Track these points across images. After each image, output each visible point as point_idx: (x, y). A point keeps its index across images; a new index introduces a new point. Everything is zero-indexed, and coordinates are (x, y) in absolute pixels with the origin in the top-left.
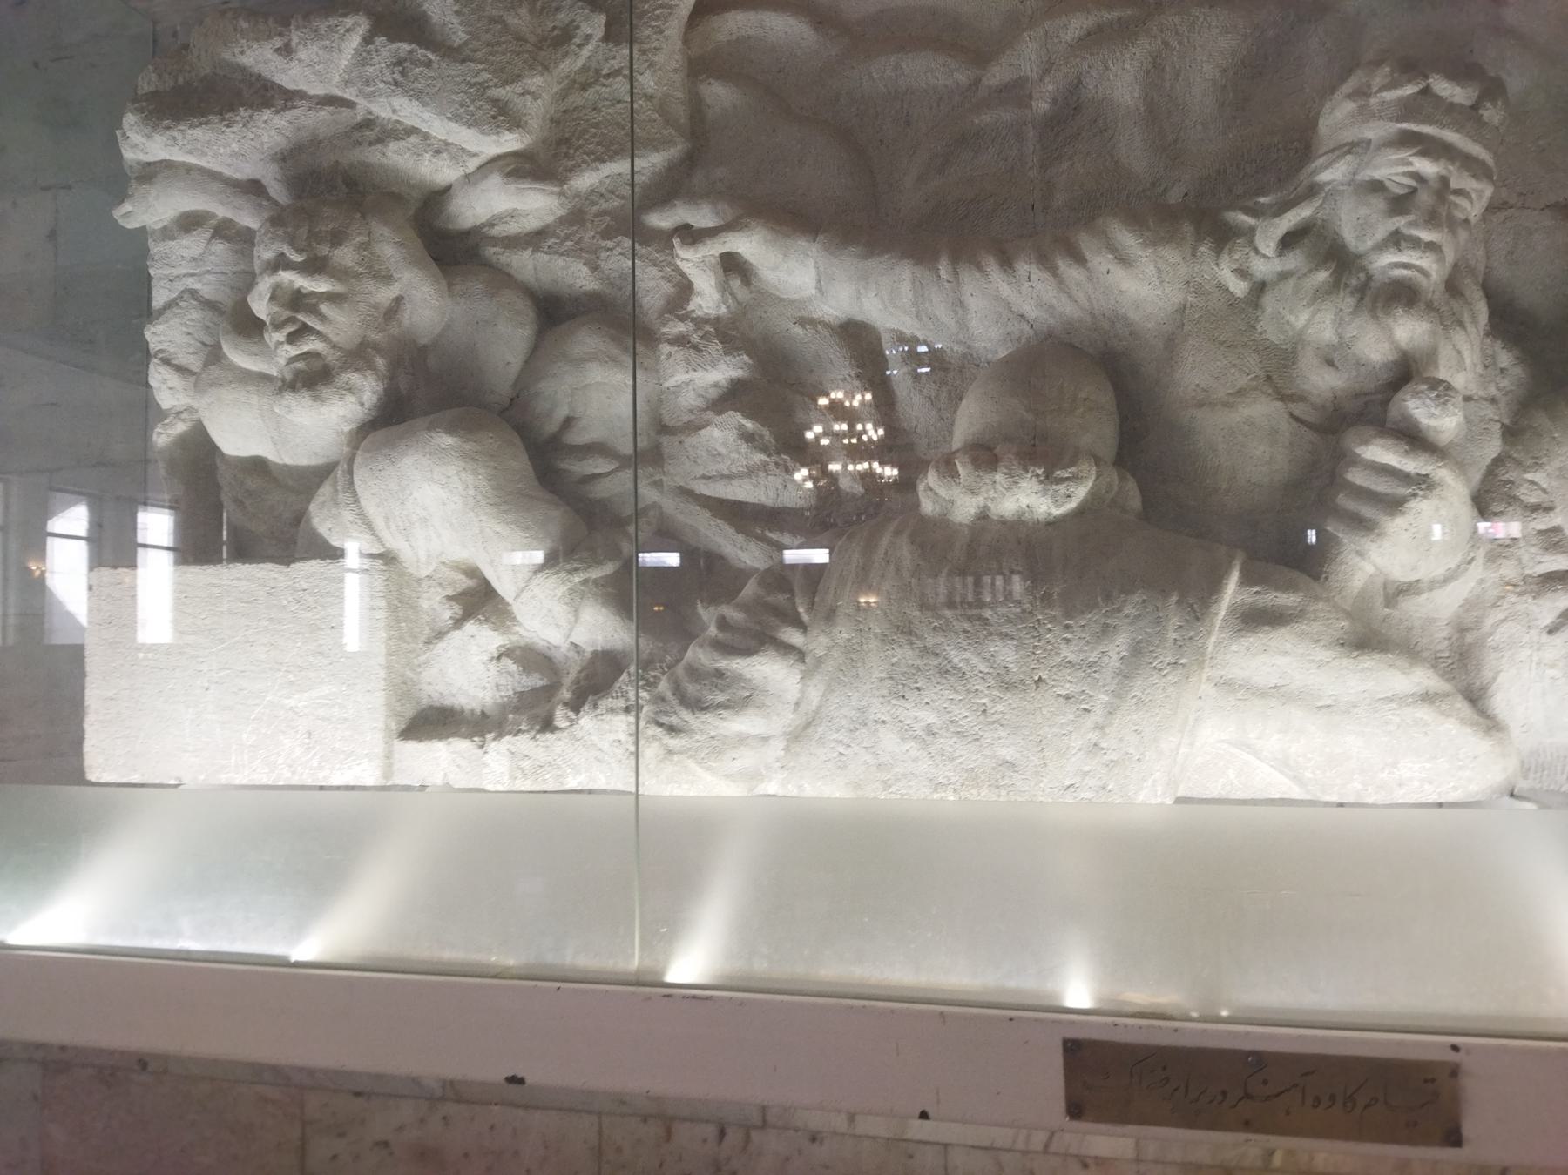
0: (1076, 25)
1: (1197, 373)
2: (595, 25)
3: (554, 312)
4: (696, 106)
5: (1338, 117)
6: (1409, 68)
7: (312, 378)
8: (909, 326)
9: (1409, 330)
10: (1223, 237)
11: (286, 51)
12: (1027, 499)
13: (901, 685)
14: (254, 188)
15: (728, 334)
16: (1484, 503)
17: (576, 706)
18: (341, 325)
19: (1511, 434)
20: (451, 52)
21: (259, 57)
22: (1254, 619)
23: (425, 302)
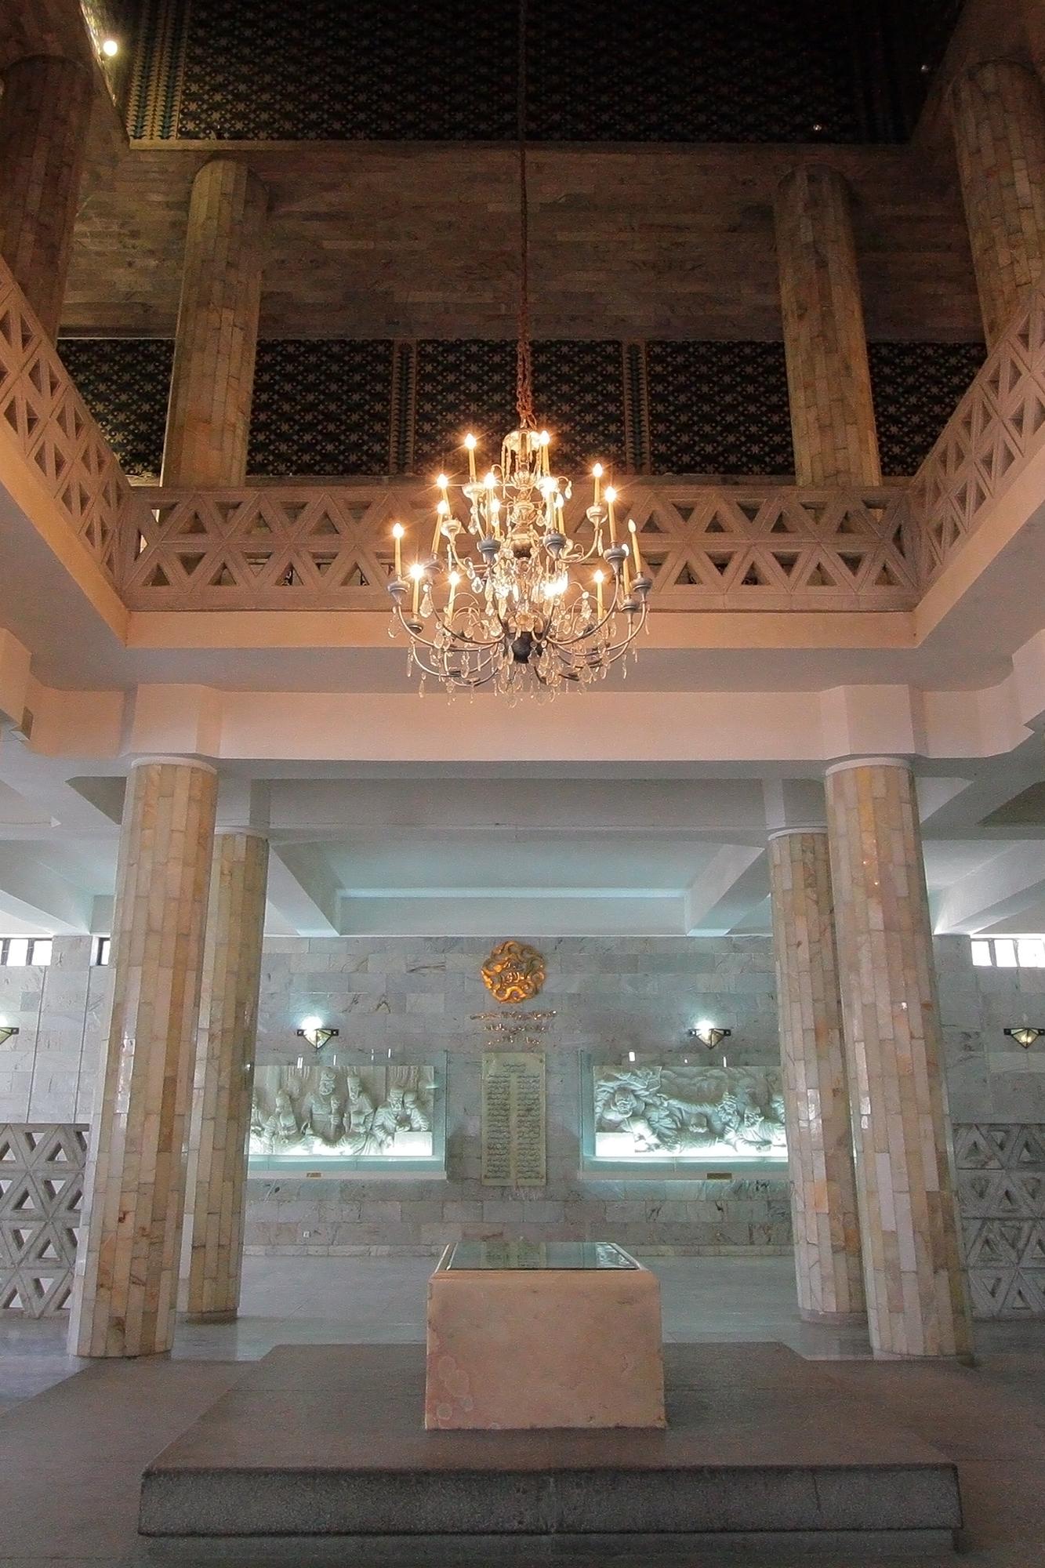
1: (714, 1119)
3: (646, 1104)
12: (701, 1130)
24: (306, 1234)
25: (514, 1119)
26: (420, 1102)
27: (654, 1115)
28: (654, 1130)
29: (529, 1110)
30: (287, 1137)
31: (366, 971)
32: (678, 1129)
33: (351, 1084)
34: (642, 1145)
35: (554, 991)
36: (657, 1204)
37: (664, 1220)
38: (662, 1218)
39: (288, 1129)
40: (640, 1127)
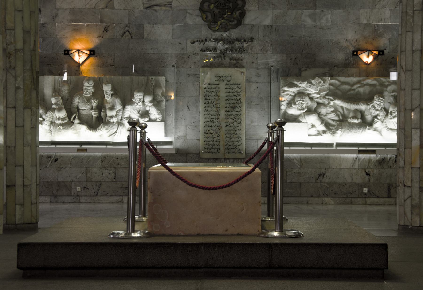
0: (358, 85)
1: (366, 113)
2: (322, 82)
3: (318, 103)
4: (329, 88)
5: (375, 98)
6: (379, 96)
7: (302, 109)
8: (346, 107)
9: (378, 112)
10: (368, 105)
11: (300, 83)
12: (356, 121)
13: (348, 132)
14: (294, 92)
15: (332, 106)
16: (382, 122)
17: (323, 134)
18: (304, 105)
19: (385, 118)
20: (314, 85)
21: (298, 83)
22: (369, 129)
23: (310, 103)
24: (78, 189)
25: (223, 113)
26: (156, 103)
27: (323, 111)
28: (323, 121)
29: (234, 108)
30: (62, 125)
31: (113, 8)
32: (340, 121)
33: (107, 89)
34: (313, 131)
35: (253, 23)
36: (323, 171)
37: (327, 181)
38: (326, 180)
39: (63, 119)
40: (313, 119)
